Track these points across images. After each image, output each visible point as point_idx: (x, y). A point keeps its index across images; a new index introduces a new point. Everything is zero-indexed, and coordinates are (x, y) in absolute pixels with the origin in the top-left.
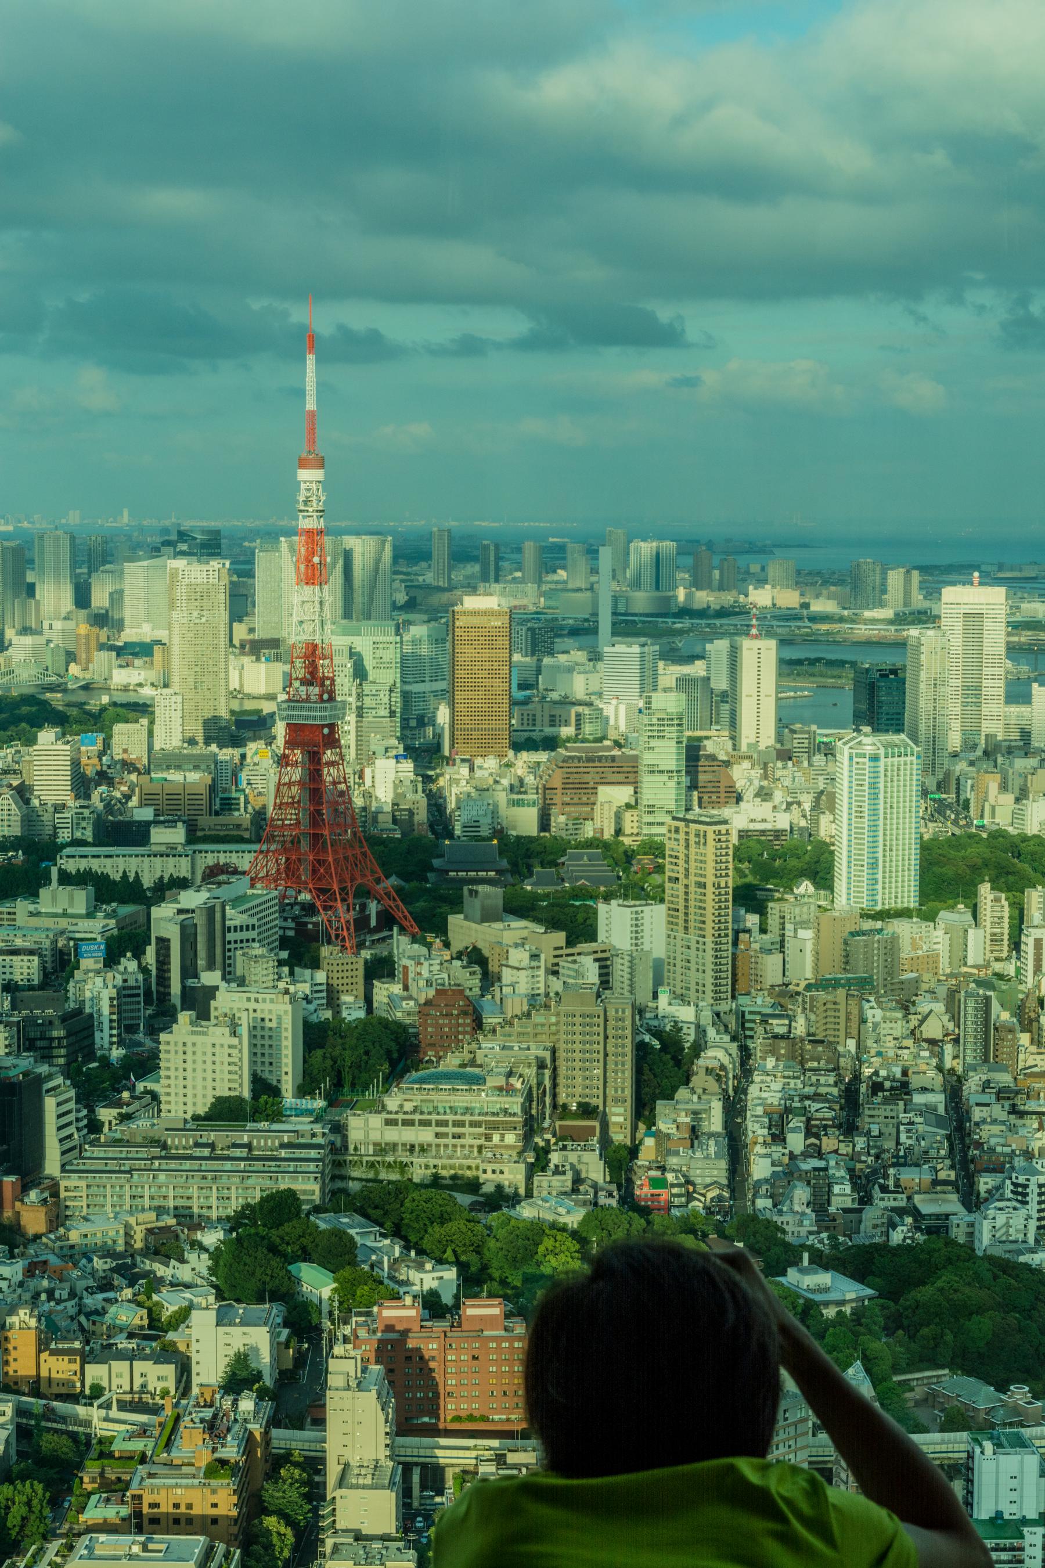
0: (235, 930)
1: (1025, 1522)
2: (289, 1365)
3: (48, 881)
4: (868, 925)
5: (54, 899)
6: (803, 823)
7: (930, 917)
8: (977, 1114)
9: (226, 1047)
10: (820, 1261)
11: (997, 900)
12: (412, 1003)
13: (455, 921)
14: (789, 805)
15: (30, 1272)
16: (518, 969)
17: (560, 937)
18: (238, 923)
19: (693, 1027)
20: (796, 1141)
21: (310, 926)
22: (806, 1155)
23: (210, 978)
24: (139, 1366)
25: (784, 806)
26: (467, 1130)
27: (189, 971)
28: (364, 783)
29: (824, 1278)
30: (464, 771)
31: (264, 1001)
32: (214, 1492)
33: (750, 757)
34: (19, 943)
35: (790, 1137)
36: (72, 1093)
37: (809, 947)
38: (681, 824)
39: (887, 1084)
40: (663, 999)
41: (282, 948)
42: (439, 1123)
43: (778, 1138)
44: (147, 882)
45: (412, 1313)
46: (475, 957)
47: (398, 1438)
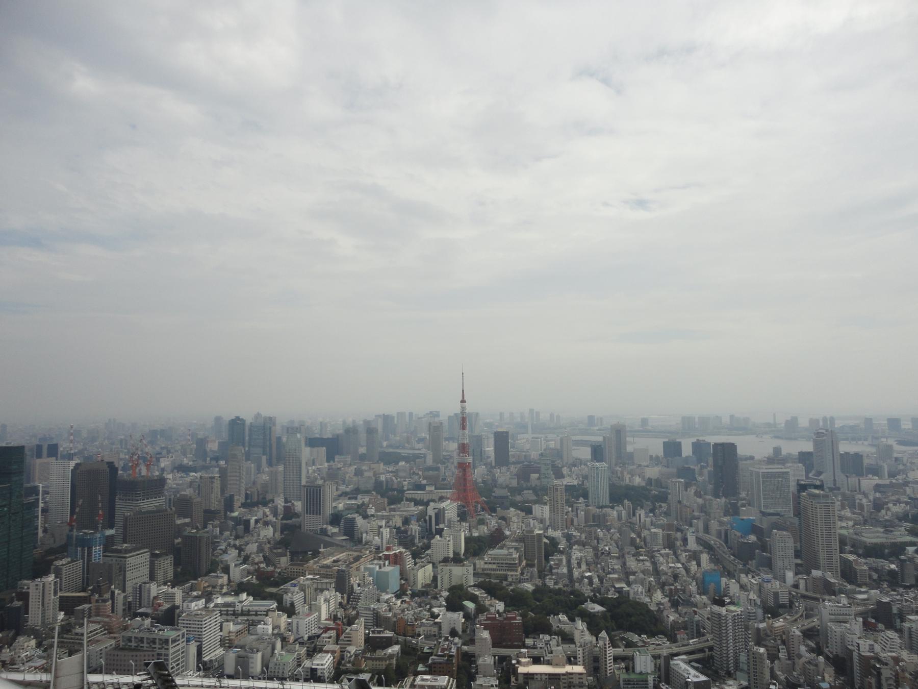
1: (648, 674)
3: (402, 500)
4: (598, 510)
10: (593, 601)
15: (402, 603)
17: (523, 514)
20: (584, 567)
22: (587, 572)
23: (441, 526)
26: (504, 565)
27: (437, 524)
30: (499, 470)
35: (582, 566)
36: (411, 556)
37: (583, 516)
40: (550, 530)
41: (458, 517)
43: (579, 566)
44: (425, 500)
45: (494, 616)
46: (503, 518)
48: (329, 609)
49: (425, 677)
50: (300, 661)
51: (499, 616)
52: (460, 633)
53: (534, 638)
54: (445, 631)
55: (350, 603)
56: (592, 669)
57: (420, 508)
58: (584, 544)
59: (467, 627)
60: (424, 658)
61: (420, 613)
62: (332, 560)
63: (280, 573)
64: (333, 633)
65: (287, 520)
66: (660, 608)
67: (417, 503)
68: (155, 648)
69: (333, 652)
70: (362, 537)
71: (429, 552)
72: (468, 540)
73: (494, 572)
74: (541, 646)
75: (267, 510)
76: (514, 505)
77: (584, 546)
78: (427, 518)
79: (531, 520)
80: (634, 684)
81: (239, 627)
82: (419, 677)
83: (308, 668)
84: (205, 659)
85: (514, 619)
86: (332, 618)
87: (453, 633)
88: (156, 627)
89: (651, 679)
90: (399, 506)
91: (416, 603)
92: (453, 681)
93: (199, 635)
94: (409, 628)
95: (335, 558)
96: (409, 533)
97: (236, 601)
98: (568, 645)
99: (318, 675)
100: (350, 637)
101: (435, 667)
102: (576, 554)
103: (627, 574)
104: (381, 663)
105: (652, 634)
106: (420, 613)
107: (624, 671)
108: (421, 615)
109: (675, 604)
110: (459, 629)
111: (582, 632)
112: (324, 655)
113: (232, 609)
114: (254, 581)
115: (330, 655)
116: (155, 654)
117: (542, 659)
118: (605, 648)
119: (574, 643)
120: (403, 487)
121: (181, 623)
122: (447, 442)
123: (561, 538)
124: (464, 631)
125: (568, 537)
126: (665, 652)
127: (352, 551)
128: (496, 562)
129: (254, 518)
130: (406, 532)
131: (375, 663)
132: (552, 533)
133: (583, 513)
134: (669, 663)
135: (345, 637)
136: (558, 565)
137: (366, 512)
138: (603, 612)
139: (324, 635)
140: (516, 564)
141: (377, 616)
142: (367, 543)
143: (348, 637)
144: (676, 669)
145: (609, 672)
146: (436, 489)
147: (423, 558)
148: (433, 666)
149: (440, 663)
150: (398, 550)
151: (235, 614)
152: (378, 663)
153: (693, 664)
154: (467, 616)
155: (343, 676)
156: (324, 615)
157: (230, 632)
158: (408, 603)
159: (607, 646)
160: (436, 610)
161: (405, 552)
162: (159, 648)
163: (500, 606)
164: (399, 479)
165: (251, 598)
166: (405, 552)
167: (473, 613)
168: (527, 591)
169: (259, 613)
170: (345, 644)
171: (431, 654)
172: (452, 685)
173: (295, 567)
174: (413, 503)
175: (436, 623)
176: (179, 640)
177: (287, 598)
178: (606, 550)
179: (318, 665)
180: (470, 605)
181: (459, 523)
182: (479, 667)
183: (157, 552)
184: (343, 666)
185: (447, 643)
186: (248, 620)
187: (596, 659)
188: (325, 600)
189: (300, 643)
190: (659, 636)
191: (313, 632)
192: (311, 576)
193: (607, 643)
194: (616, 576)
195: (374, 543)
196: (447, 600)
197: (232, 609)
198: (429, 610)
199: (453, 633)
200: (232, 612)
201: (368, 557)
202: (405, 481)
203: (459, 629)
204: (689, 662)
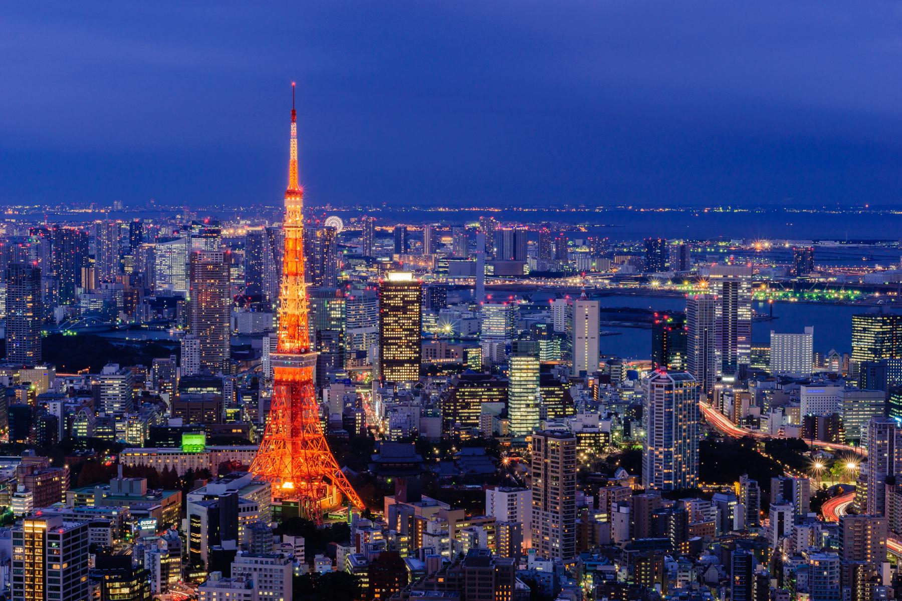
0: (244, 511)
3: (116, 475)
5: (120, 487)
9: (243, 596)
11: (752, 485)
12: (364, 562)
16: (433, 536)
18: (246, 505)
19: (552, 576)
21: (292, 505)
23: (228, 545)
25: (604, 415)
28: (322, 399)
31: (267, 563)
33: (582, 381)
38: (542, 438)
41: (274, 520)
174: (144, 482)
181: (277, 538)
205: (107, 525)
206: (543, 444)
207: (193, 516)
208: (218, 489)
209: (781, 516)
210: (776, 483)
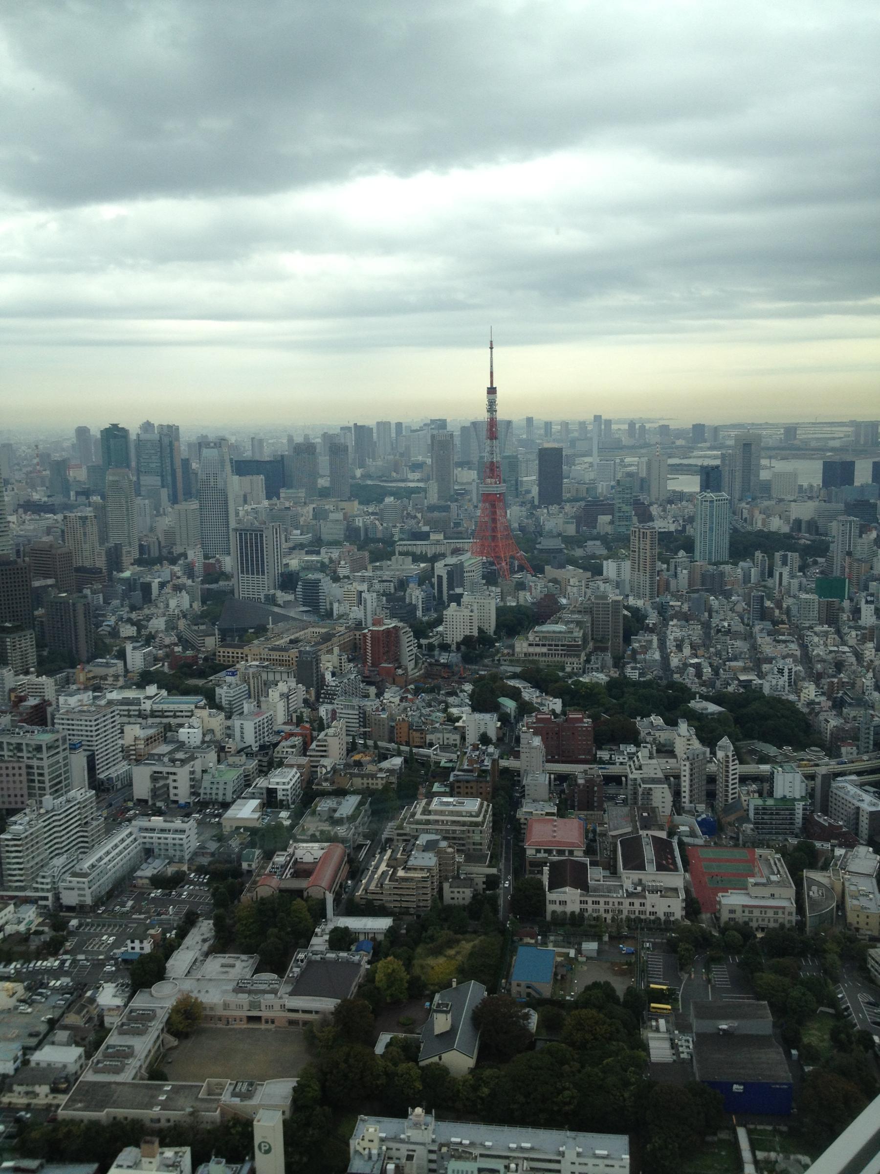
1: (795, 799)
2: (501, 735)
4: (710, 567)
5: (397, 561)
6: (680, 528)
7: (736, 564)
8: (759, 641)
13: (548, 568)
14: (674, 522)
15: (401, 701)
17: (589, 574)
18: (468, 569)
20: (687, 651)
23: (458, 590)
24: (446, 735)
26: (560, 648)
27: (451, 587)
29: (705, 704)
30: (545, 511)
32: (481, 782)
34: (385, 578)
35: (684, 650)
36: (412, 634)
37: (687, 577)
39: (723, 630)
40: (631, 598)
42: (550, 645)
46: (555, 581)
47: (547, 764)
48: (288, 708)
49: (445, 799)
50: (249, 780)
51: (555, 718)
52: (494, 739)
53: (611, 750)
54: (472, 737)
55: (321, 700)
56: (704, 793)
57: (422, 565)
58: (686, 618)
59: (504, 734)
60: (443, 774)
61: (430, 715)
62: (288, 639)
63: (206, 659)
64: (297, 740)
65: (209, 583)
66: (813, 709)
67: (417, 558)
68: (23, 757)
69: (299, 766)
70: (332, 609)
71: (440, 629)
72: (501, 612)
73: (543, 659)
74: (621, 760)
75: (176, 568)
76: (573, 562)
77: (687, 621)
78: (435, 580)
79: (600, 583)
80: (772, 814)
81: (151, 732)
82: (436, 799)
83: (261, 788)
84: (102, 776)
85: (580, 720)
86: (294, 720)
87: (485, 739)
88: (21, 728)
89: (799, 807)
90: (389, 563)
91: (424, 700)
92: (488, 805)
93: (89, 741)
94: (417, 735)
95: (292, 637)
96: (407, 601)
97: (142, 696)
98: (665, 760)
99: (279, 798)
100: (325, 746)
101: (459, 787)
102: (674, 631)
103: (758, 662)
104: (375, 781)
105: (800, 746)
106: (430, 715)
107: (756, 795)
108: (433, 717)
109: (838, 705)
110: (492, 734)
111: (689, 740)
112: (286, 770)
113: (137, 708)
114: (166, 669)
115: (295, 770)
116: (23, 766)
117: (624, 779)
118: (727, 762)
119: (675, 757)
120: (392, 535)
121: (59, 724)
122: (460, 469)
123: (650, 610)
124: (499, 739)
125: (662, 610)
126: (822, 770)
127: (319, 627)
128: (547, 643)
129: (157, 581)
130: (403, 599)
131: (365, 781)
132: (634, 602)
133: (685, 572)
134: (829, 786)
135: (317, 746)
136: (646, 649)
137: (335, 572)
138: (720, 713)
139: (283, 743)
140: (578, 646)
141: (364, 718)
142: (340, 617)
143: (322, 746)
144: (842, 794)
145: (731, 797)
146: (445, 538)
147: (432, 637)
148: (457, 785)
149: (467, 782)
150: (391, 623)
151: (141, 715)
152: (370, 781)
153: (867, 788)
154: (504, 719)
155: (317, 799)
156: (281, 717)
157: (136, 739)
158: (412, 701)
159: (731, 759)
160: (454, 711)
161: (404, 628)
162: (28, 758)
163: (557, 704)
164: (385, 525)
165: (164, 693)
166: (404, 628)
167: (513, 714)
168: (597, 684)
169: (178, 714)
170: (317, 756)
171: (453, 769)
172: (486, 811)
173: (231, 650)
174: (410, 558)
175: (456, 728)
176: (58, 747)
177: (223, 693)
178: (724, 627)
179: (278, 783)
180: (509, 705)
182: (526, 788)
183: (7, 624)
184: (317, 784)
185: (477, 753)
186: (161, 723)
187: (712, 779)
188: (282, 695)
189: (247, 754)
190: (813, 748)
191: (266, 739)
192: (257, 663)
193: (730, 754)
194: (740, 664)
195: (352, 616)
196: (471, 697)
197: (137, 708)
198: (445, 710)
199: (485, 739)
200: (137, 713)
201: (346, 636)
202: (395, 526)
203: (492, 734)
204: (861, 786)
205: (391, 581)
206: (637, 534)
207: (438, 576)
208: (452, 560)
209: (781, 574)
210: (778, 555)
